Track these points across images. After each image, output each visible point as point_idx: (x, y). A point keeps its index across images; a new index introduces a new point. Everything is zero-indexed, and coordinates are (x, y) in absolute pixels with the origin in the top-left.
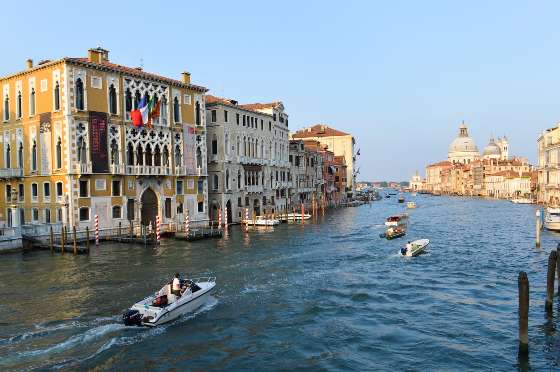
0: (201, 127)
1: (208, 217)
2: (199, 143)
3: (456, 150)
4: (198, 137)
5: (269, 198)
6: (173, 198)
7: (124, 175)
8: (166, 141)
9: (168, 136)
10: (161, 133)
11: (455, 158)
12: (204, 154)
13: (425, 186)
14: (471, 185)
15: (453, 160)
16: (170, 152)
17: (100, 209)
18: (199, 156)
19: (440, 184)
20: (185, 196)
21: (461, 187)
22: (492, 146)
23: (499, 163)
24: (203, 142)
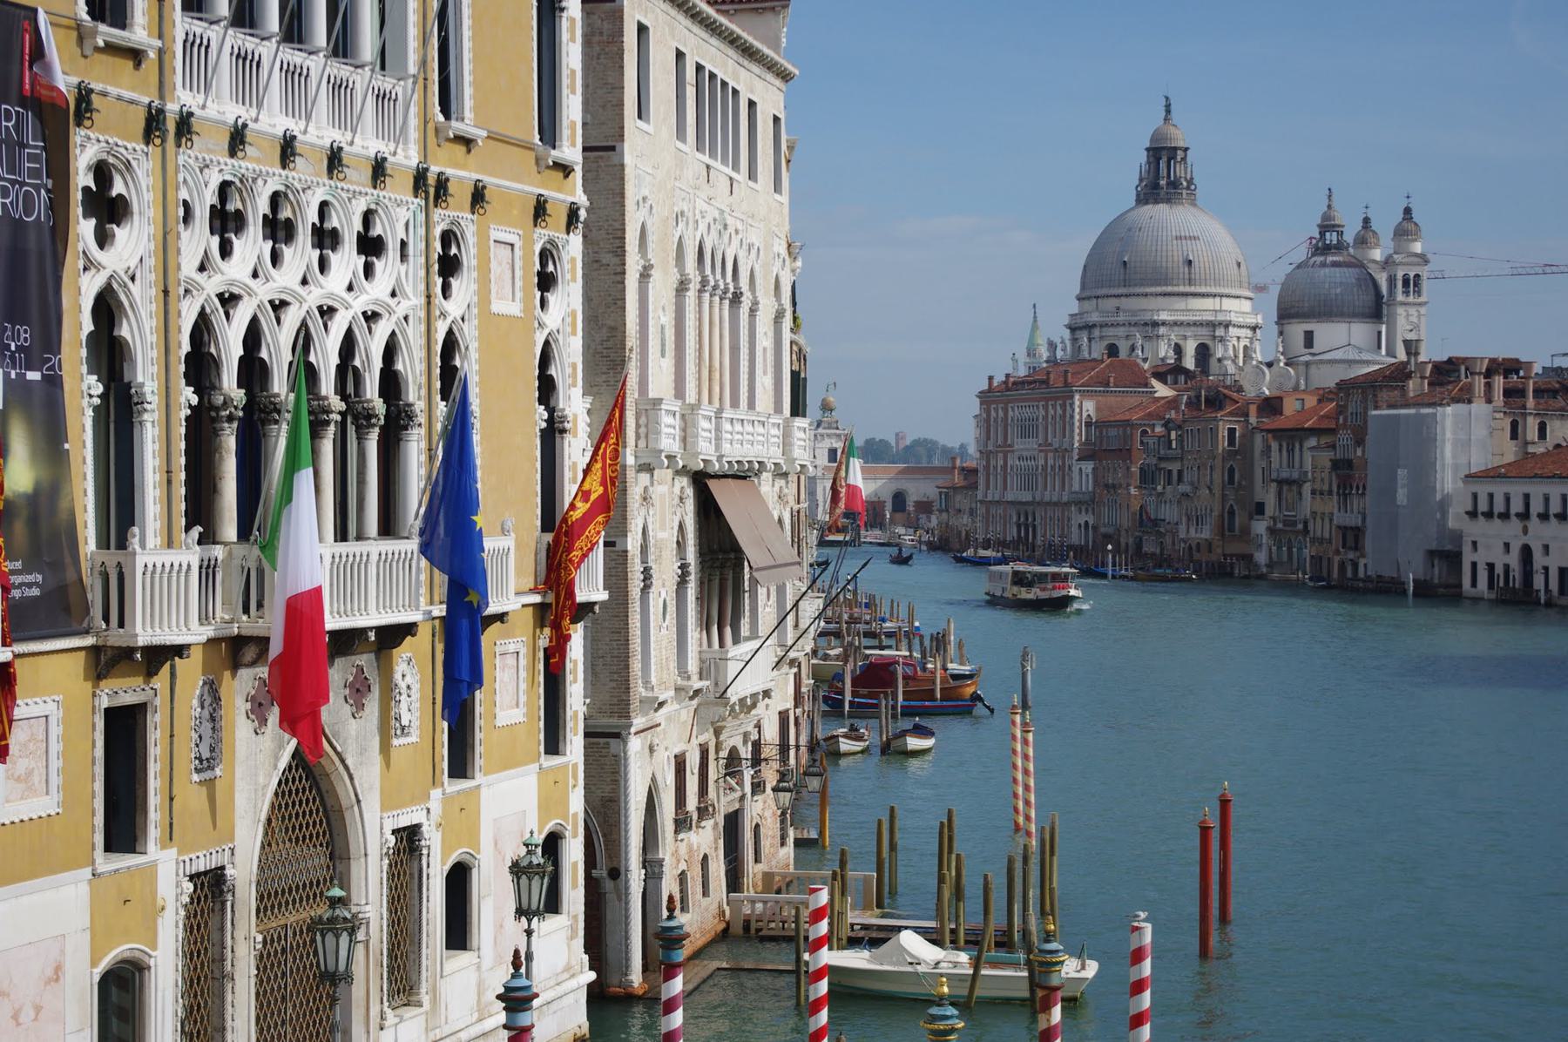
0: (565, 169)
1: (586, 958)
2: (543, 303)
3: (1126, 283)
4: (545, 255)
5: (771, 733)
6: (426, 816)
7: (179, 650)
8: (393, 294)
9: (403, 244)
10: (368, 218)
11: (1121, 331)
12: (575, 403)
13: (972, 512)
14: (1344, 529)
15: (1106, 343)
16: (414, 395)
17: (15, 1017)
18: (552, 433)
19: (1087, 503)
20: (484, 792)
21: (1246, 531)
22: (1335, 264)
23: (1538, 392)
24: (568, 299)
